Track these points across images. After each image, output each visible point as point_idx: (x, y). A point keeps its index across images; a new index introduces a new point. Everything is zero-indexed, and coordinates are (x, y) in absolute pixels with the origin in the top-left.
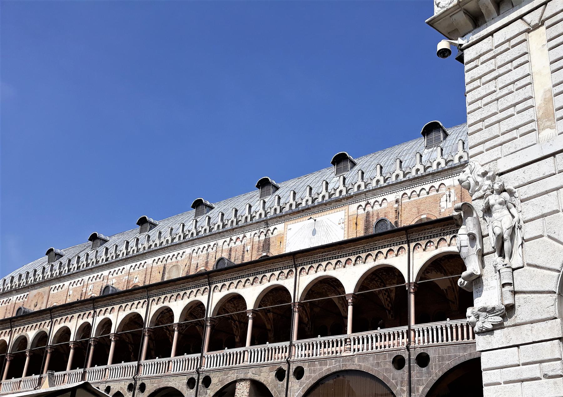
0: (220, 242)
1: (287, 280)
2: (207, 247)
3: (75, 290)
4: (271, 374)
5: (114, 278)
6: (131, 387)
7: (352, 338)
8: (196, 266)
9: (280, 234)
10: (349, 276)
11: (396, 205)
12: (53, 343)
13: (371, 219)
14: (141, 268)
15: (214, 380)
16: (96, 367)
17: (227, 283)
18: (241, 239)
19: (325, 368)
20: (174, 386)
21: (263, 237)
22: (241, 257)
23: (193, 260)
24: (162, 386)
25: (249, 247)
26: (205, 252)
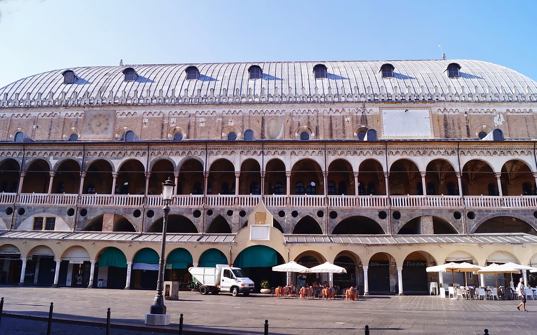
0: (321, 110)
1: (449, 157)
2: (307, 111)
3: (150, 119)
4: (450, 214)
5: (202, 117)
6: (320, 214)
7: (505, 199)
8: (298, 123)
9: (377, 115)
10: (497, 163)
11: (466, 115)
12: (210, 170)
13: (448, 120)
14: (235, 115)
15: (402, 214)
16: (274, 196)
17: (401, 151)
18: (340, 111)
19: (490, 214)
20: (366, 216)
21: (360, 114)
22: (342, 124)
23: (294, 118)
24: (353, 215)
25: (349, 119)
26: (305, 114)
